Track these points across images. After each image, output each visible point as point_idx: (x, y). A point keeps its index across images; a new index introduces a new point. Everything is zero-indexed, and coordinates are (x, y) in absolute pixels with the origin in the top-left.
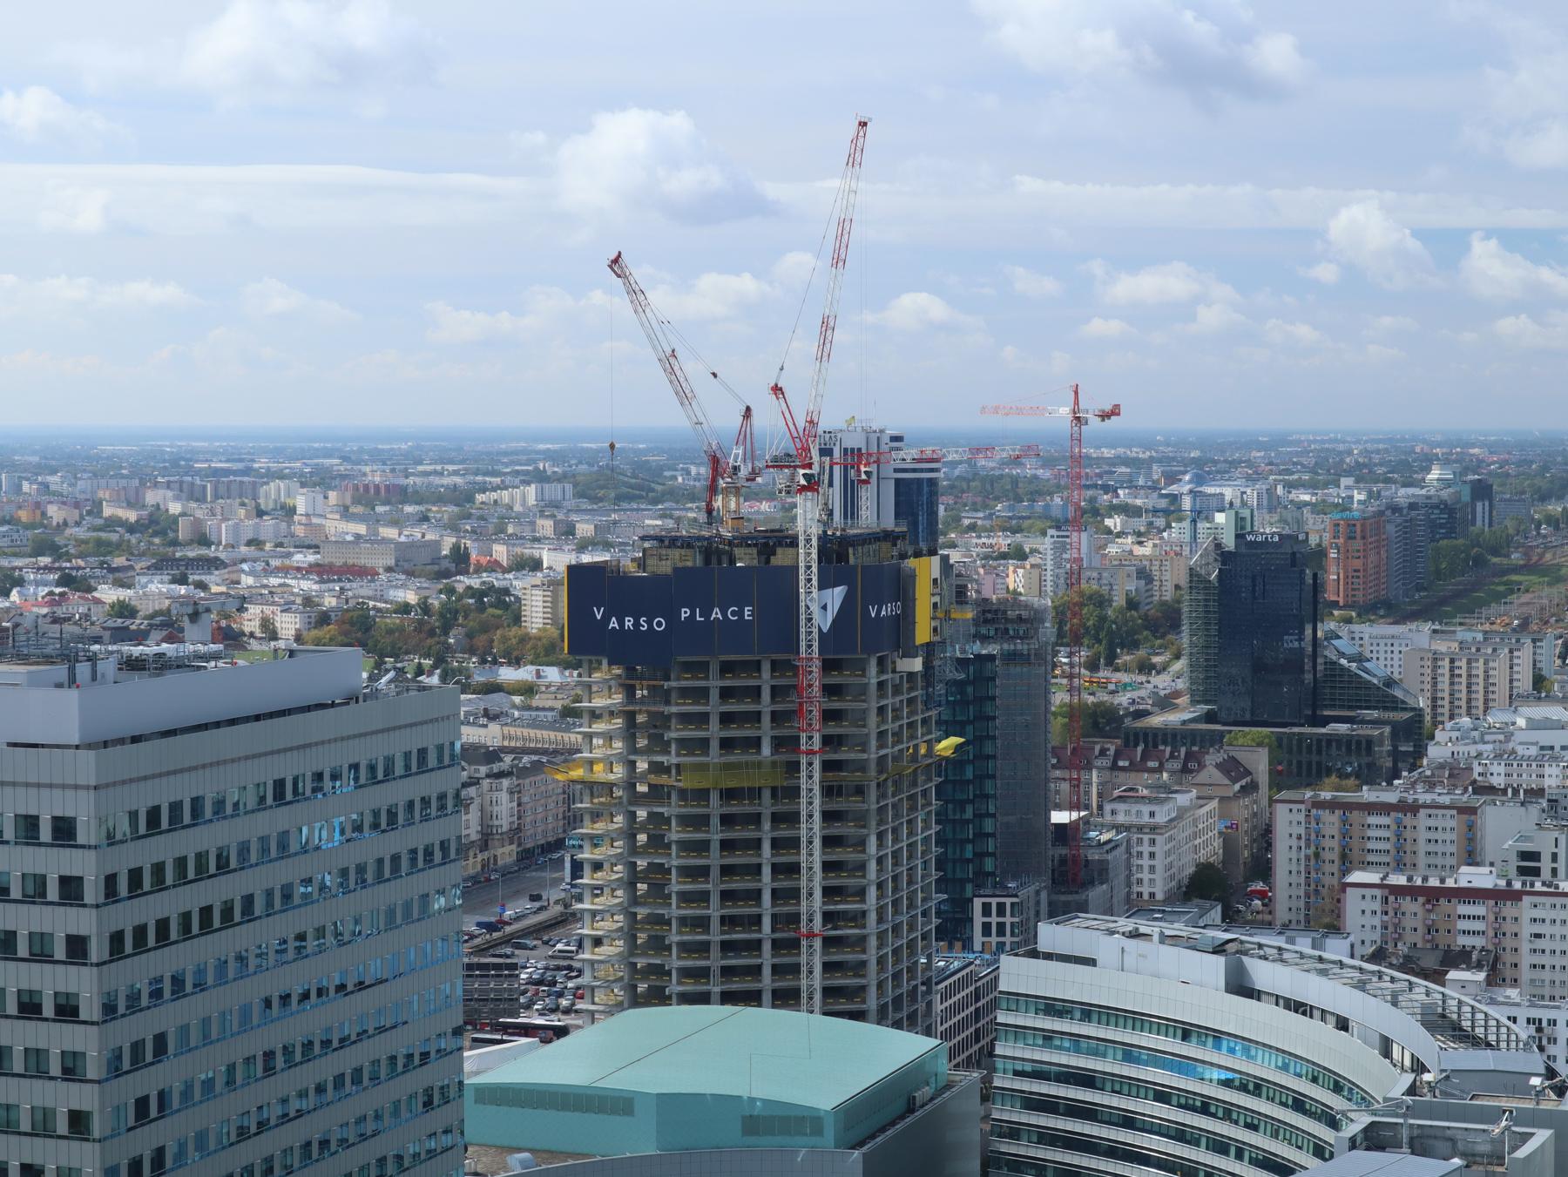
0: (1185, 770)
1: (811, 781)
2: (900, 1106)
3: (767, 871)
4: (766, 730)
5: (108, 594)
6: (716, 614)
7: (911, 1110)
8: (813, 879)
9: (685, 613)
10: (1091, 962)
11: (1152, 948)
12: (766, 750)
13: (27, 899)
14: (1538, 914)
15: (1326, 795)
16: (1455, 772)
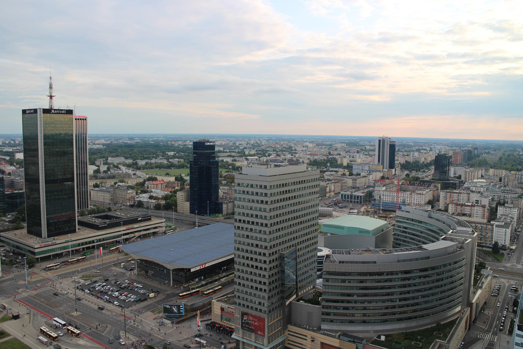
16: (468, 188)
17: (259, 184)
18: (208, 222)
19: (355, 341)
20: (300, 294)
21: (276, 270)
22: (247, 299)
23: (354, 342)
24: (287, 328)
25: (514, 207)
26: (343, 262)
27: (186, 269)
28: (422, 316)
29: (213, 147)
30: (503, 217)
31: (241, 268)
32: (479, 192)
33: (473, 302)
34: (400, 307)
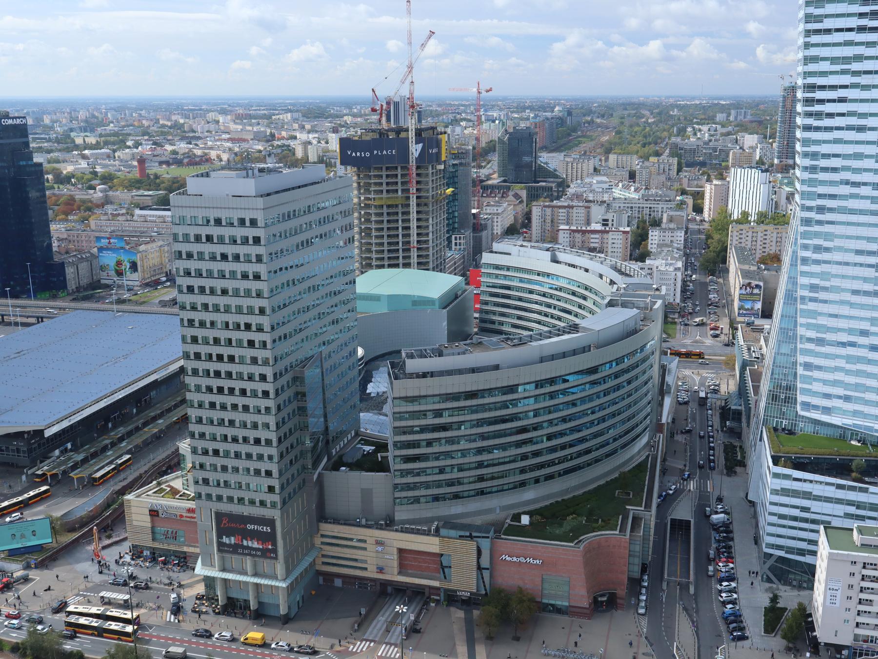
0: (503, 197)
1: (413, 201)
2: (454, 297)
3: (400, 229)
4: (400, 187)
5: (169, 148)
6: (385, 152)
7: (456, 297)
8: (414, 231)
9: (375, 152)
10: (509, 254)
11: (528, 250)
12: (400, 193)
13: (243, 244)
14: (614, 237)
15: (547, 204)
16: (578, 196)
17: (235, 216)
18: (41, 312)
19: (474, 534)
20: (334, 451)
21: (289, 409)
22: (225, 482)
23: (471, 537)
24: (318, 530)
25: (678, 228)
26: (432, 374)
27: (29, 432)
28: (589, 465)
29: (21, 131)
30: (666, 249)
31: (205, 414)
32: (605, 202)
33: (664, 420)
34: (553, 450)
